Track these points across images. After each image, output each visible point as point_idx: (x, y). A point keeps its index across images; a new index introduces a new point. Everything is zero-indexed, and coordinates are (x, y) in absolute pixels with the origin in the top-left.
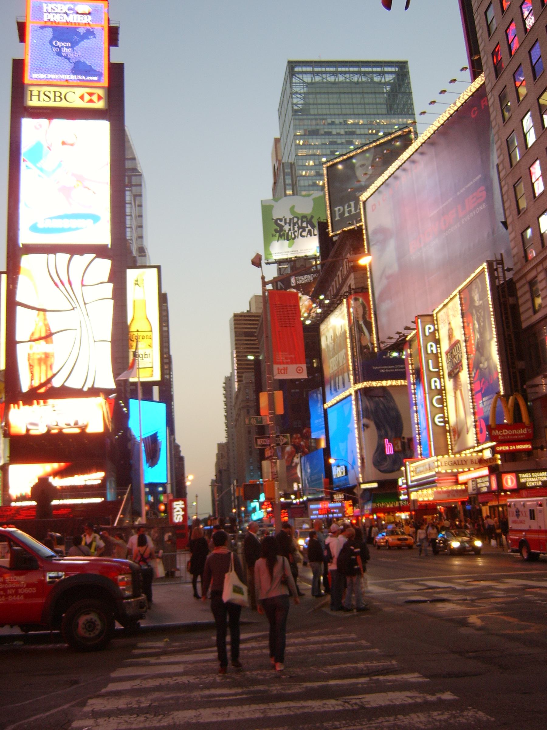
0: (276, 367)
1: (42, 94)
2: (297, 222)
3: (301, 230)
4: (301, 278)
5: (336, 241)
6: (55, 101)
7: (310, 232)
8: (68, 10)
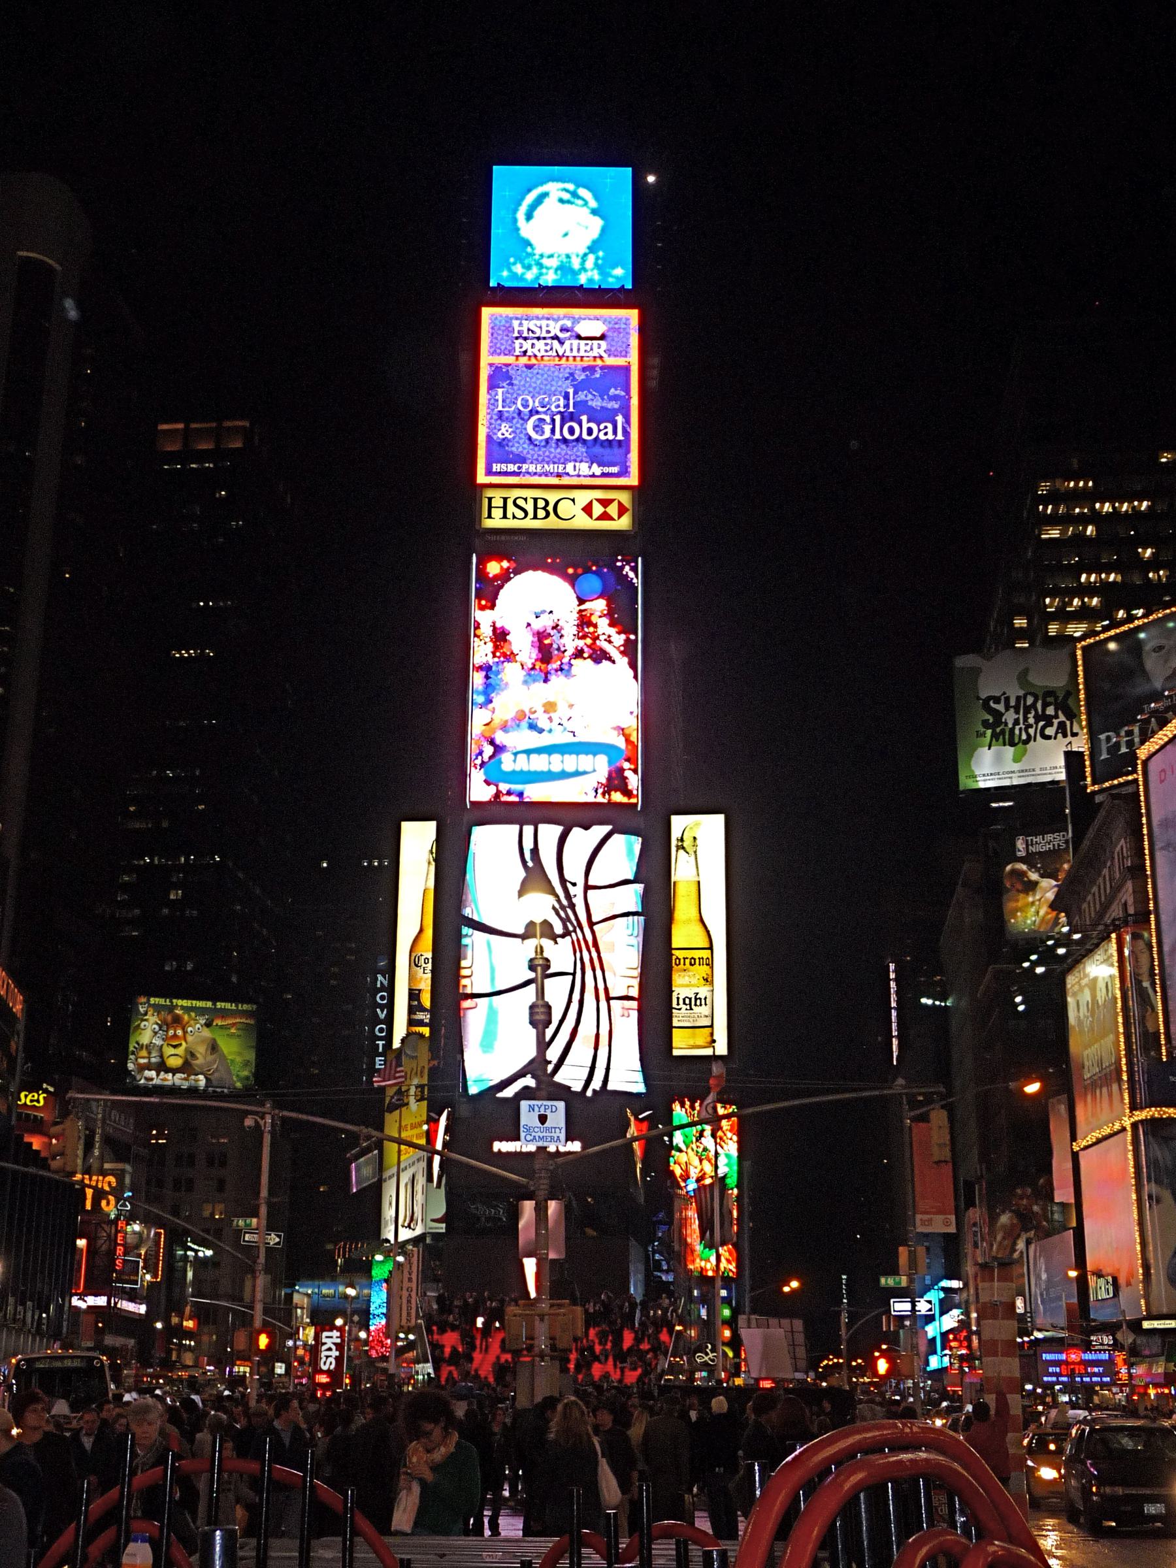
0: (918, 1217)
1: (510, 503)
2: (1034, 705)
3: (1041, 724)
4: (1039, 839)
5: (1101, 804)
6: (535, 517)
7: (1062, 726)
8: (562, 330)
